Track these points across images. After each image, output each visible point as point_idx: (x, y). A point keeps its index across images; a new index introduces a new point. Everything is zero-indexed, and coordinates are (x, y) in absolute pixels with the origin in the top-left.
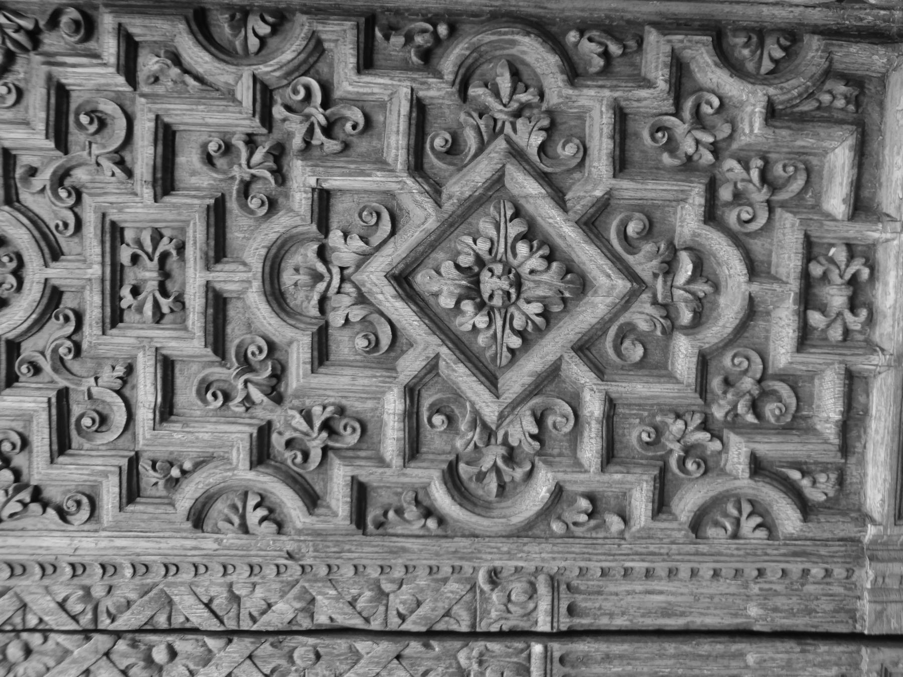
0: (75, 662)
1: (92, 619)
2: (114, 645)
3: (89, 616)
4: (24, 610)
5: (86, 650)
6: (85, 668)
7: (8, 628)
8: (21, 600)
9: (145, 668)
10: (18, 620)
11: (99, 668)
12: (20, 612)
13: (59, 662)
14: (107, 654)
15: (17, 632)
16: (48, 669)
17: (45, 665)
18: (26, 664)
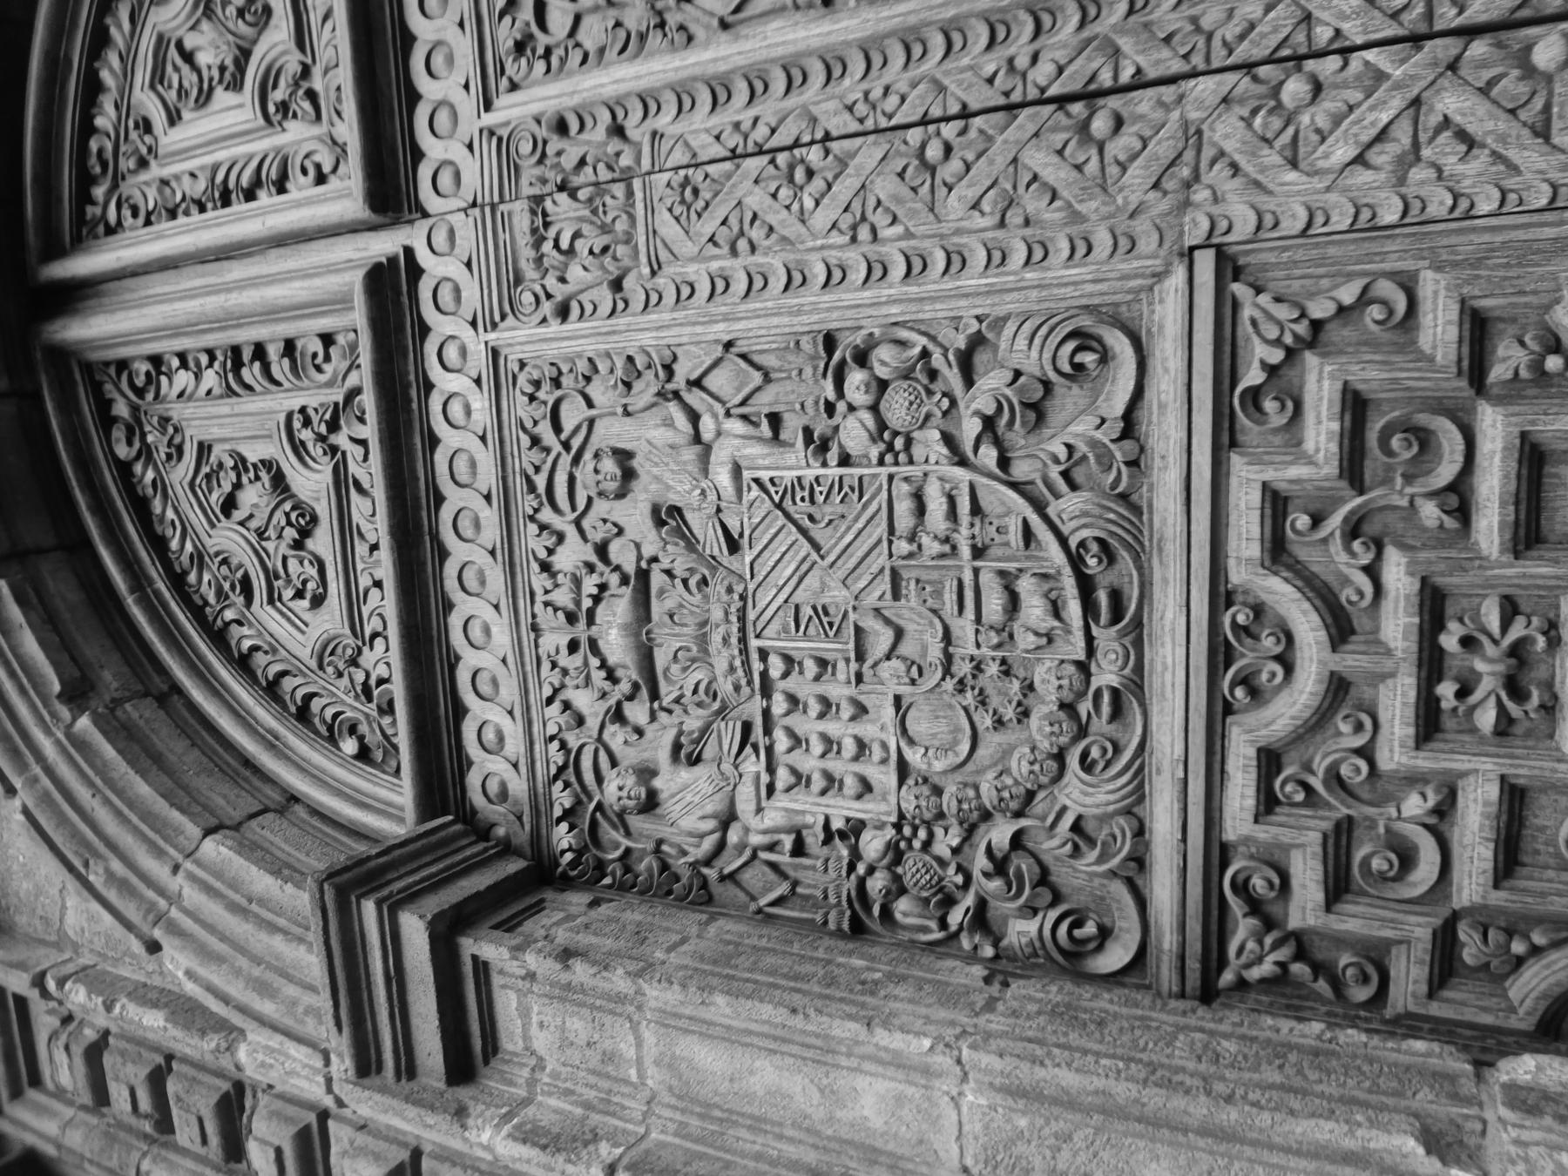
0: (1398, 86)
1: (1423, 14)
2: (1465, 50)
3: (1419, 9)
4: (1309, 24)
5: (1415, 65)
6: (1416, 92)
7: (1286, 52)
8: (1303, 9)
9: (1521, 79)
10: (1300, 37)
11: (1438, 92)
12: (1304, 26)
13: (1368, 97)
14: (1453, 66)
15: (1299, 59)
16: (1351, 108)
17: (1346, 102)
18: (1313, 109)
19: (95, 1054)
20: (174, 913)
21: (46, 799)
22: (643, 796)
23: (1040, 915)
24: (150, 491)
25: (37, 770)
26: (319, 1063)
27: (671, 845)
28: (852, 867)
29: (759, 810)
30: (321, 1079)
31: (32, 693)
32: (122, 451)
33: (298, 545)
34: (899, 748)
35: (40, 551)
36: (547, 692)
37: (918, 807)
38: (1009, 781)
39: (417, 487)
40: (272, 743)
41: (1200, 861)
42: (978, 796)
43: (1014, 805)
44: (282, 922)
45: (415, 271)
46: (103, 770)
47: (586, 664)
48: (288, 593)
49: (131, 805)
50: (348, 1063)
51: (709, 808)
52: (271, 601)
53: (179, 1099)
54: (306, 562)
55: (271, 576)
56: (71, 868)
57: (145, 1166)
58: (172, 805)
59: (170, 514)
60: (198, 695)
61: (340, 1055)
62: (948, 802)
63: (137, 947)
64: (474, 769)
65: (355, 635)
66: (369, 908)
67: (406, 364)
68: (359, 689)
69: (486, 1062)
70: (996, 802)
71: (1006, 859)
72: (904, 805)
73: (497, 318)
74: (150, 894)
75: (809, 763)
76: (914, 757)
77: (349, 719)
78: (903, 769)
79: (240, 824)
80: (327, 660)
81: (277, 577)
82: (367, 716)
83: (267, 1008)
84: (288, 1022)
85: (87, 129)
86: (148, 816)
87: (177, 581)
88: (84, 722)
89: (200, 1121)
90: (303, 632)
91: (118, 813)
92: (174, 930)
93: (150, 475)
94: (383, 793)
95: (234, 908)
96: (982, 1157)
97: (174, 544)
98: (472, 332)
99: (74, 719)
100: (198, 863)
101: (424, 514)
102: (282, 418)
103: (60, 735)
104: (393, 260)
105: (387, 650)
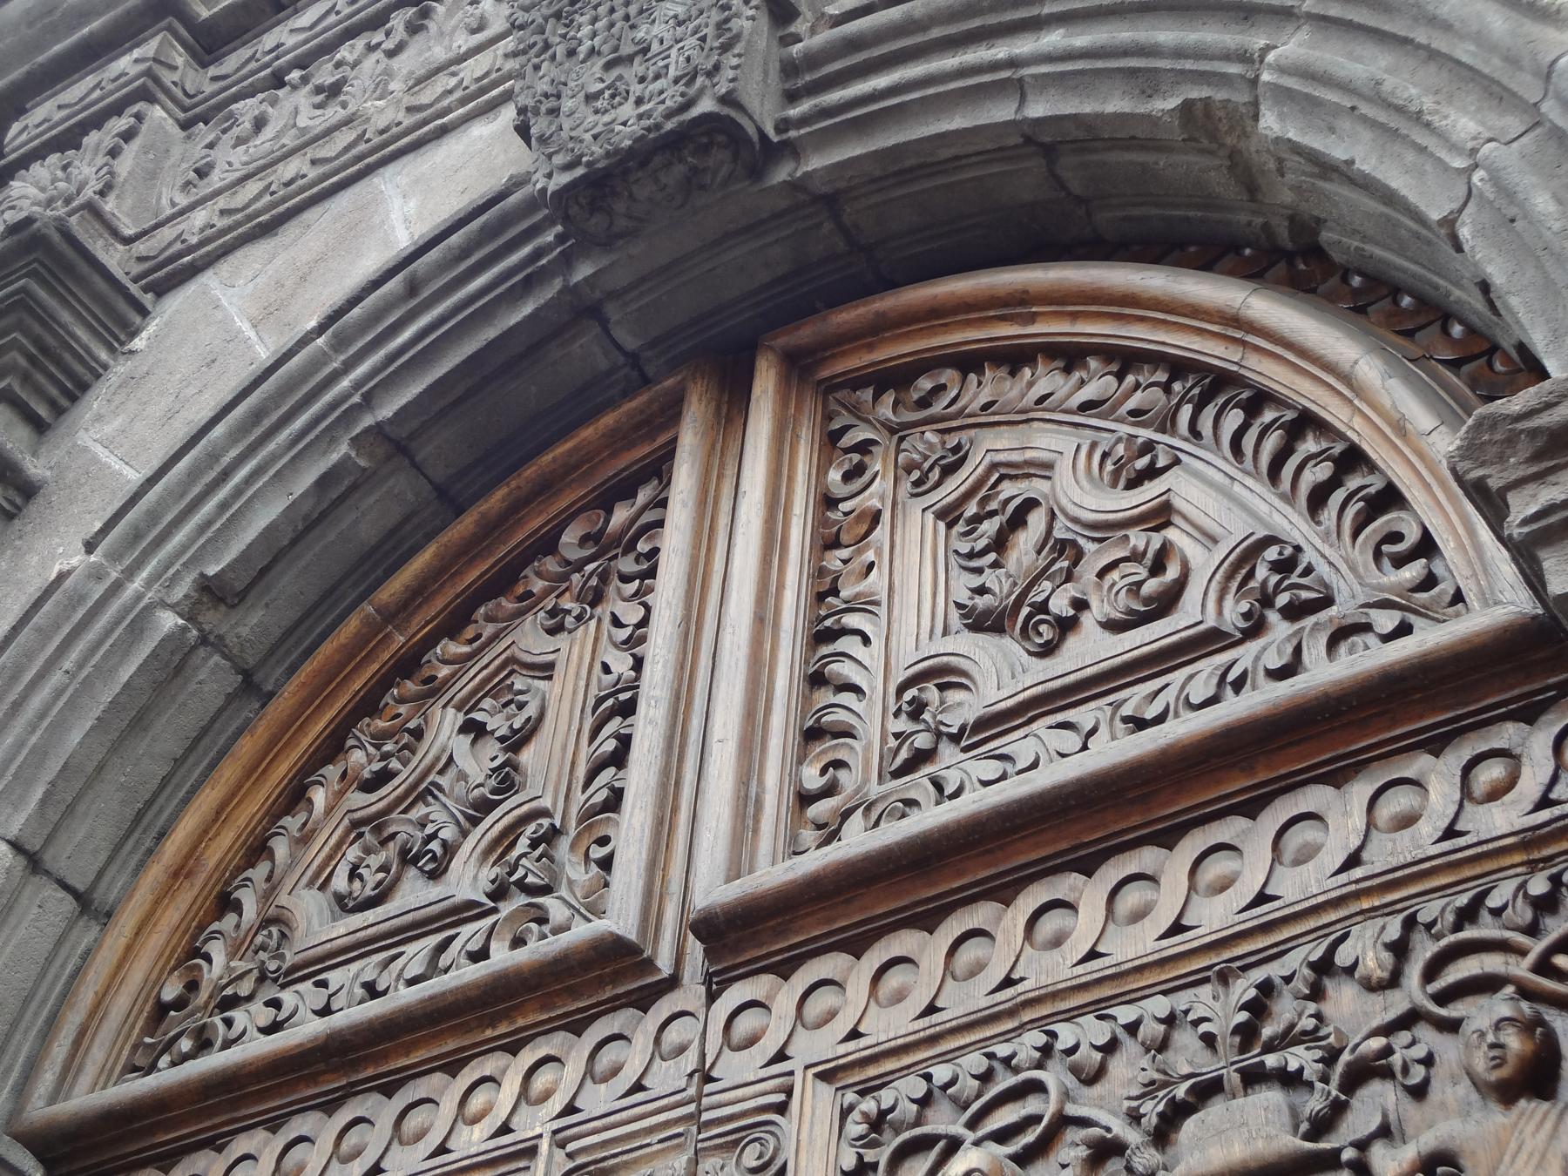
21: (77, 599)
24: (520, 590)
31: (202, 541)
32: (570, 537)
35: (416, 466)
39: (399, 1056)
40: (181, 872)
45: (643, 1001)
46: (104, 671)
54: (381, 875)
55: (377, 822)
58: (53, 784)
60: (247, 747)
67: (535, 1011)
68: (229, 991)
73: (571, 1147)
79: (47, 873)
80: (274, 930)
85: (969, 362)
86: (40, 754)
87: (408, 664)
88: (169, 621)
90: (310, 884)
91: (42, 715)
93: (538, 585)
94: (97, 1055)
98: (558, 1108)
101: (370, 1072)
102: (546, 802)
104: (649, 965)
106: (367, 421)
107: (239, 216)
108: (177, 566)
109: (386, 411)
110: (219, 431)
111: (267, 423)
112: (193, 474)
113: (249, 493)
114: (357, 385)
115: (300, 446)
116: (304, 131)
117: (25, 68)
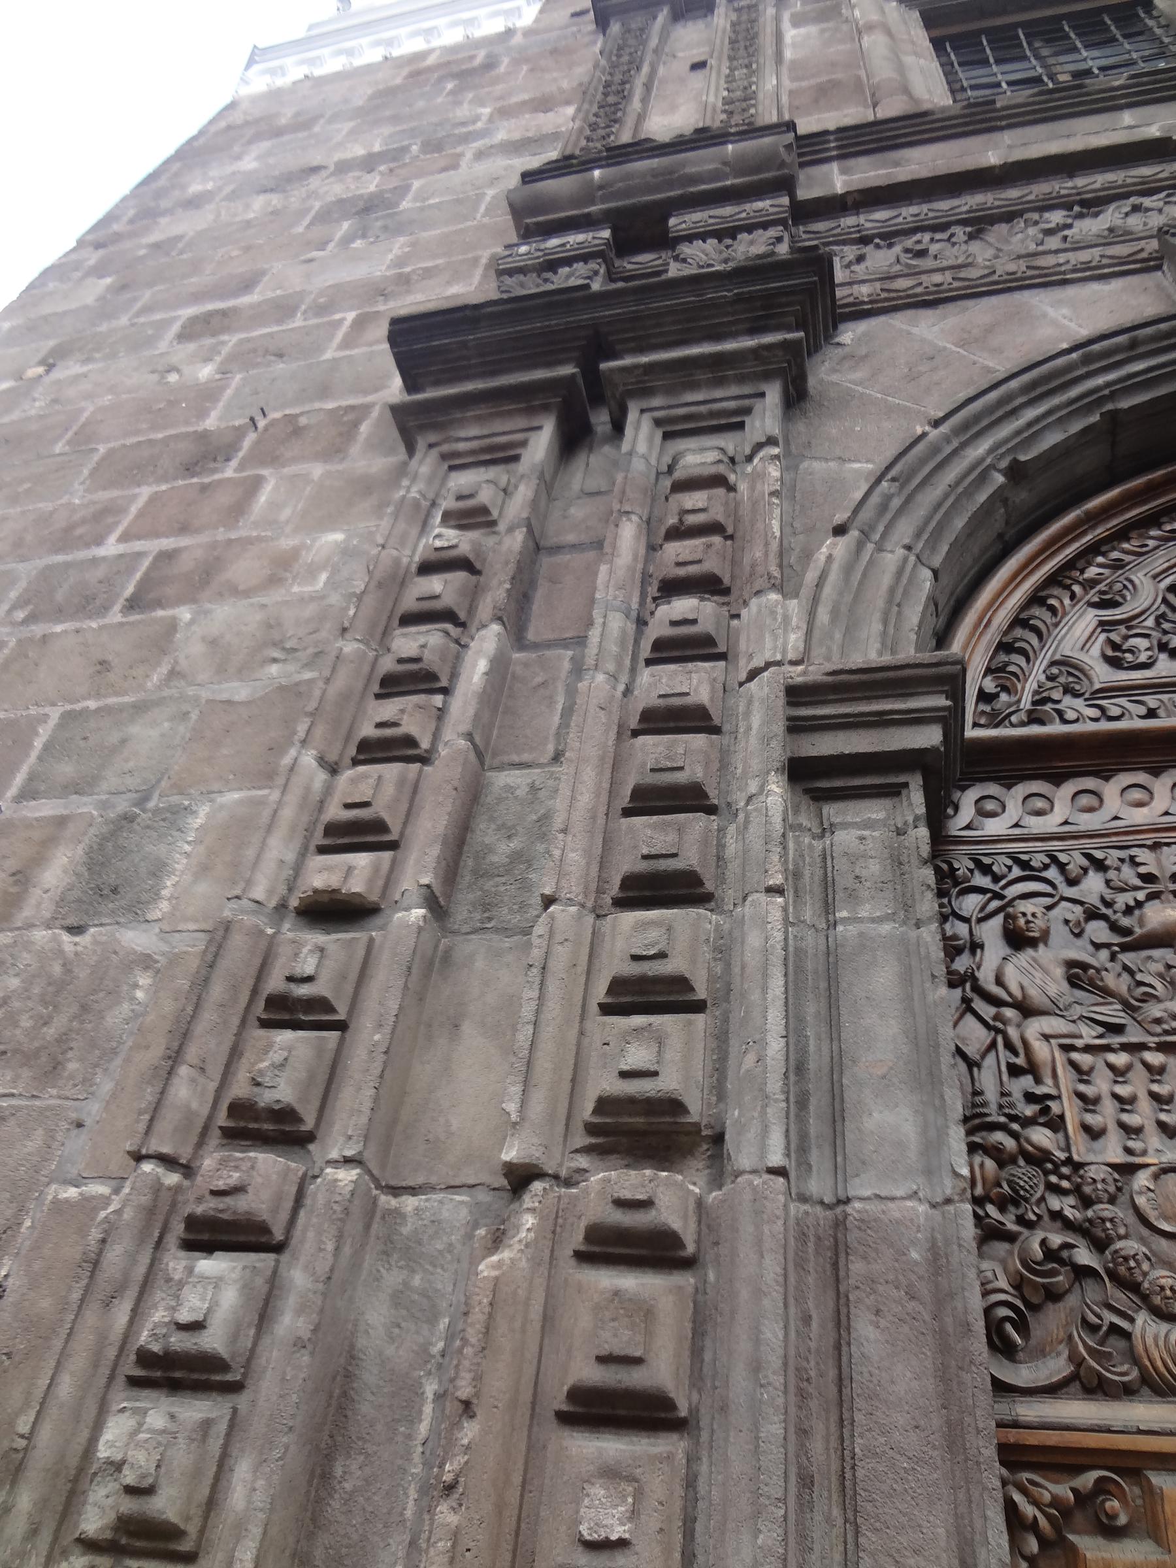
19: (718, 481)
20: (870, 547)
21: (935, 449)
22: (1031, 934)
23: (1011, 1290)
24: (1168, 527)
25: (955, 443)
26: (791, 656)
27: (981, 958)
28: (1013, 1118)
29: (1047, 1037)
30: (778, 657)
33: (1163, 647)
34: (1148, 1165)
36: (1099, 854)
37: (1094, 1181)
38: (1145, 1266)
40: (983, 624)
41: (1123, 1447)
42: (1120, 1238)
43: (1122, 1269)
44: (891, 631)
46: (969, 493)
47: (1136, 888)
48: (1115, 637)
49: (946, 514)
50: (800, 680)
51: (1033, 992)
52: (1101, 623)
53: (709, 546)
54: (1150, 653)
56: (888, 468)
57: (634, 518)
59: (1152, 543)
61: (804, 673)
62: (1105, 1210)
63: (840, 518)
64: (1004, 790)
65: (1093, 693)
66: (942, 701)
69: (807, 791)
70: (1123, 1253)
71: (1062, 1262)
72: (1093, 1167)
74: (881, 528)
75: (1101, 1084)
76: (1142, 1179)
77: (1015, 686)
78: (1127, 1170)
80: (1063, 669)
81: (1129, 628)
82: (1019, 701)
83: (823, 616)
84: (817, 634)
87: (1094, 549)
88: (1000, 479)
89: (699, 562)
90: (1082, 649)
91: (939, 505)
92: (860, 546)
95: (892, 591)
96: (865, 1216)
97: (1126, 546)
99: (999, 471)
100: (915, 566)
103: (989, 461)
105: (1092, 719)
106: (1110, 406)
107: (967, 283)
108: (1003, 449)
109: (1125, 404)
110: (1014, 384)
111: (1039, 391)
112: (1001, 402)
113: (1044, 423)
114: (1108, 385)
115: (1074, 407)
116: (908, 266)
117: (679, 192)
